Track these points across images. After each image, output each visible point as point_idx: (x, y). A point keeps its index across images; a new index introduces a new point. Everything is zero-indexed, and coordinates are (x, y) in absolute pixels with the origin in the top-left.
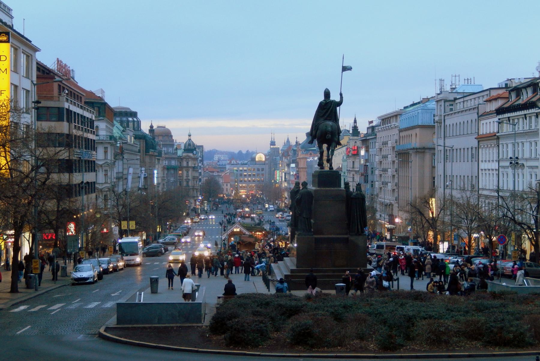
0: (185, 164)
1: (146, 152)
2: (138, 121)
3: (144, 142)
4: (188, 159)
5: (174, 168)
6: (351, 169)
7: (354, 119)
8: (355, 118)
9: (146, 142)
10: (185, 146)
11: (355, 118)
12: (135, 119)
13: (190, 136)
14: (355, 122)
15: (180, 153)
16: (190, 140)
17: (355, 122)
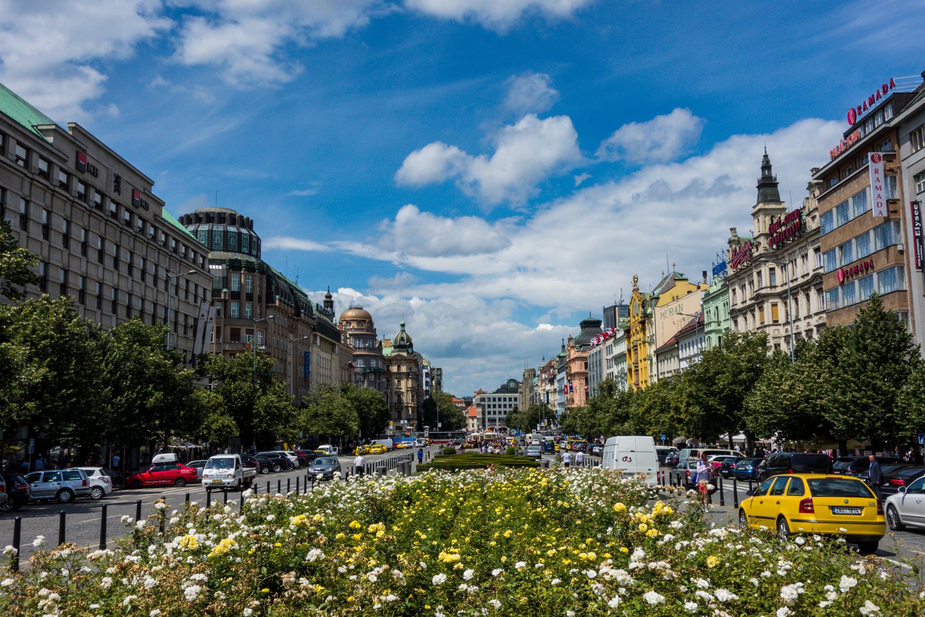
0: (394, 369)
1: (267, 302)
2: (251, 236)
3: (264, 280)
4: (400, 360)
5: (377, 372)
6: (763, 292)
7: (762, 158)
8: (766, 156)
9: (267, 279)
10: (396, 341)
11: (766, 156)
12: (244, 231)
13: (403, 325)
14: (766, 166)
15: (387, 351)
16: (404, 331)
17: (766, 166)
